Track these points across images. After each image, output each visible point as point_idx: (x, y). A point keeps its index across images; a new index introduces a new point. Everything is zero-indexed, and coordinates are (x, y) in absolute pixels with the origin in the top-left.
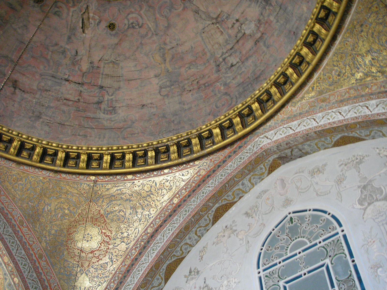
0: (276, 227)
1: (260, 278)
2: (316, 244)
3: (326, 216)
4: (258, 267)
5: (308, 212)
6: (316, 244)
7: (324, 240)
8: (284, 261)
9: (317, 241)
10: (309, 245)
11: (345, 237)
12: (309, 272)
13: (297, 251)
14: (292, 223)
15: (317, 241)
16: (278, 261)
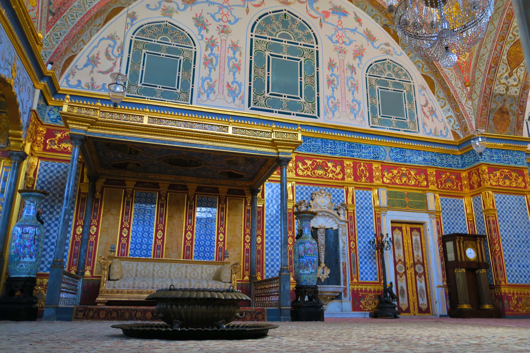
0: (273, 12)
1: (252, 40)
2: (297, 44)
3: (310, 31)
4: (252, 31)
5: (298, 19)
6: (297, 44)
7: (304, 45)
8: (272, 39)
9: (300, 43)
10: (293, 41)
11: (317, 52)
12: (288, 58)
13: (284, 40)
14: (285, 18)
15: (300, 43)
16: (268, 37)
